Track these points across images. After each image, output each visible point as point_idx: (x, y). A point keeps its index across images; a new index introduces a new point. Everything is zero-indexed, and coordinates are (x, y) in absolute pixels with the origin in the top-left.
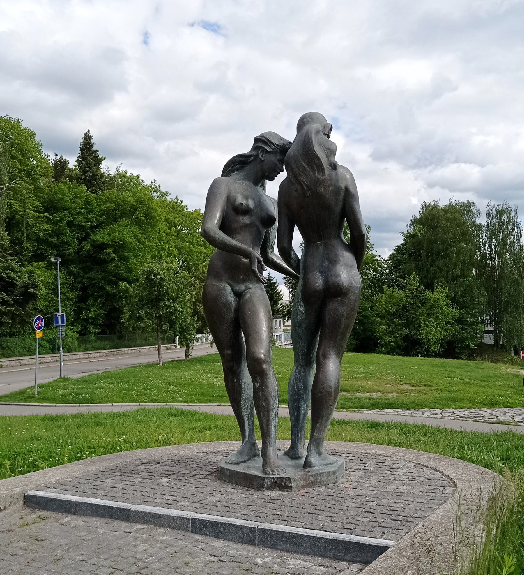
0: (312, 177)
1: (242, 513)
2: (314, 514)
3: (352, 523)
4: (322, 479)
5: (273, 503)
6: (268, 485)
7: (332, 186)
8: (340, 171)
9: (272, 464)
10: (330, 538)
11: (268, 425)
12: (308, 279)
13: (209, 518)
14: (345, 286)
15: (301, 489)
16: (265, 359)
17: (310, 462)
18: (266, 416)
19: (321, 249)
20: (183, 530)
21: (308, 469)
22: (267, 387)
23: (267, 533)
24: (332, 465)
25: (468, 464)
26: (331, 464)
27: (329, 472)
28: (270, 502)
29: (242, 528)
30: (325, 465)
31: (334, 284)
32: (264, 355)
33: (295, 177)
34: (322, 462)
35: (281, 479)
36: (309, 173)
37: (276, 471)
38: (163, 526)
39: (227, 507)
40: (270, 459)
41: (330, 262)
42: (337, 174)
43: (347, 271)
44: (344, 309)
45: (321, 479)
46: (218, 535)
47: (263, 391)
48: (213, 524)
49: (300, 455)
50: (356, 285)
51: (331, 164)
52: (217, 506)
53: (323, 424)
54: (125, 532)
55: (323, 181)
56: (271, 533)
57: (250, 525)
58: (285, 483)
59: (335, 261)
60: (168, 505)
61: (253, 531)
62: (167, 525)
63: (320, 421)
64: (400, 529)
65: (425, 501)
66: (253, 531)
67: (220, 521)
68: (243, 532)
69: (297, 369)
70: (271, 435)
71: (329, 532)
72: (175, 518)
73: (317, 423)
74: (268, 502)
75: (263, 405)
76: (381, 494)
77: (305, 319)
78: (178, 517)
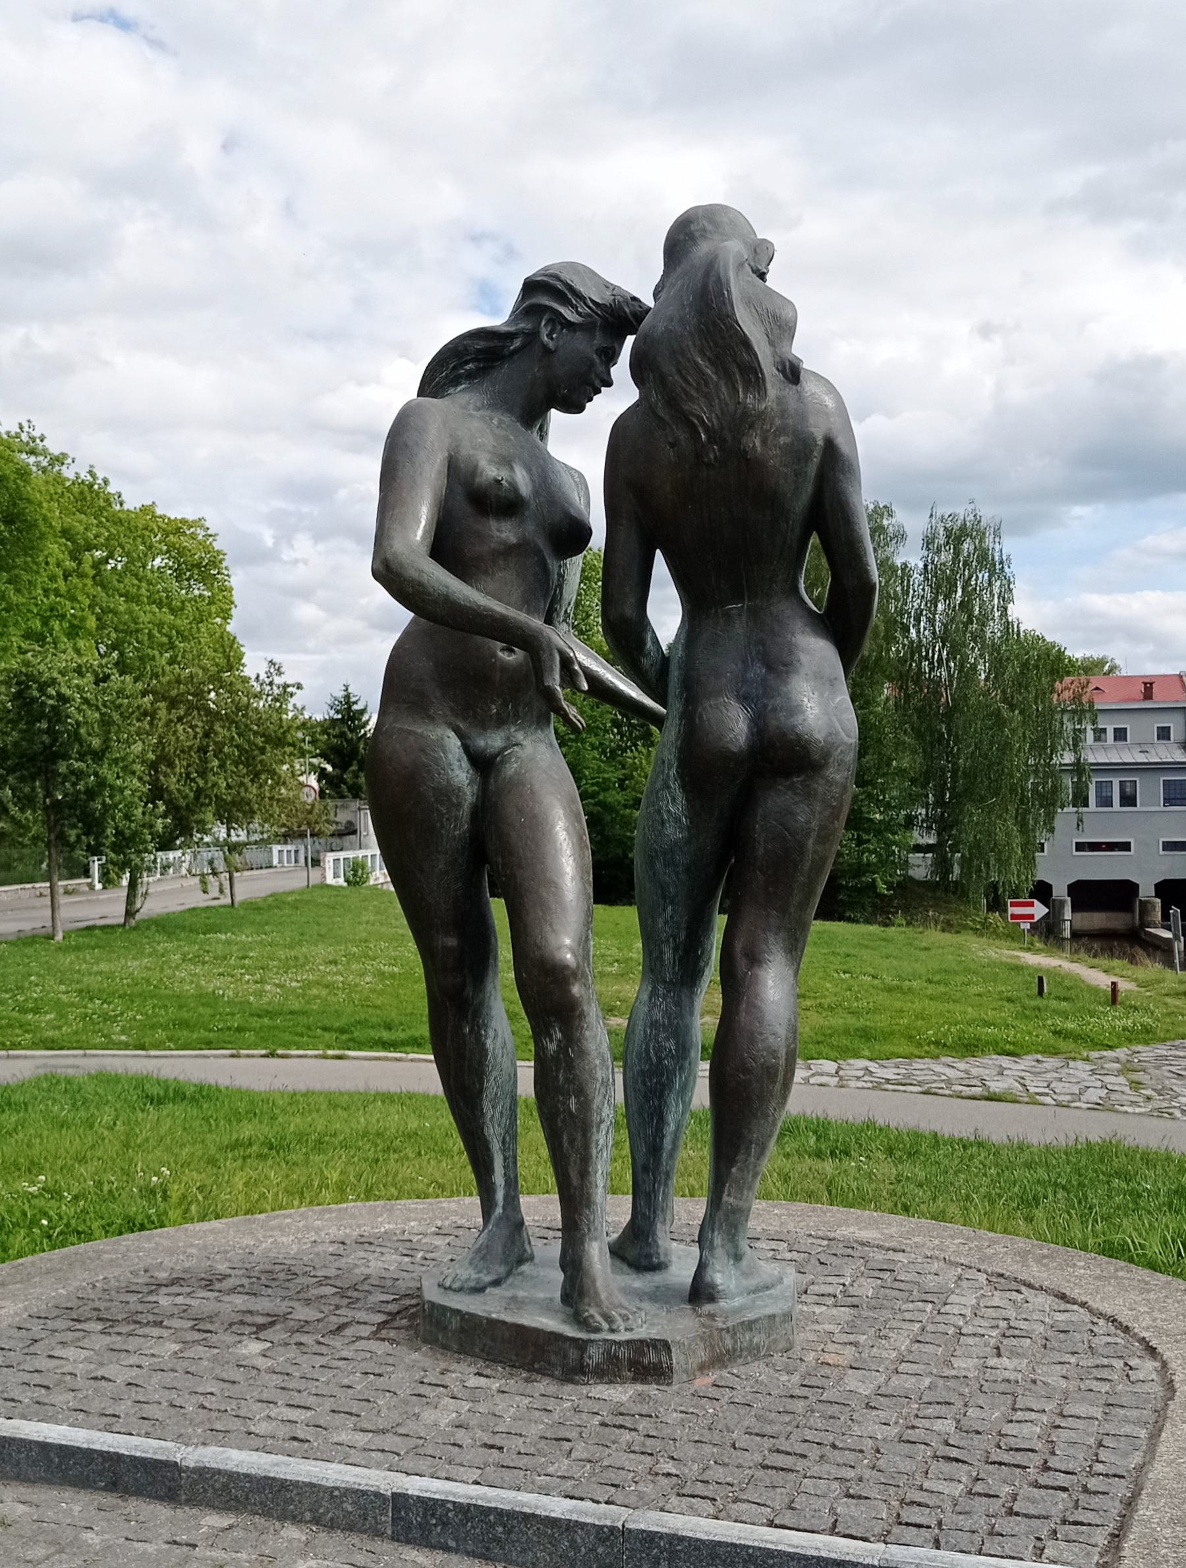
0: (727, 405)
1: (551, 1470)
2: (782, 1469)
3: (919, 1504)
4: (755, 1340)
5: (631, 1430)
6: (597, 1364)
7: (787, 434)
8: (809, 387)
9: (603, 1297)
10: (876, 1563)
11: (584, 1174)
12: (701, 717)
13: (454, 1495)
14: (817, 741)
15: (698, 1373)
16: (578, 967)
17: (713, 1286)
18: (579, 1143)
19: (740, 628)
20: (365, 1532)
21: (708, 1308)
22: (582, 1053)
23: (658, 1547)
24: (772, 1291)
25: (1145, 1273)
26: (768, 1288)
27: (774, 1316)
28: (621, 1427)
29: (569, 1527)
30: (754, 1292)
31: (784, 734)
32: (574, 954)
33: (672, 402)
34: (745, 1283)
35: (640, 1346)
36: (717, 386)
37: (619, 1321)
38: (296, 1519)
39: (492, 1447)
40: (594, 1282)
41: (770, 668)
42: (800, 398)
43: (821, 695)
44: (813, 813)
45: (751, 1340)
46: (488, 1549)
47: (570, 1066)
48: (468, 1512)
49: (662, 1258)
50: (846, 739)
51: (784, 367)
52: (460, 1446)
53: (751, 1167)
54: (175, 1543)
55: (761, 415)
56: (671, 1544)
57: (599, 1519)
58: (651, 1357)
59: (785, 665)
60: (298, 1444)
61: (608, 1539)
62: (308, 1516)
63: (740, 1157)
64: (1082, 1524)
65: (1098, 1412)
66: (608, 1539)
67: (493, 1505)
68: (573, 1542)
69: (653, 994)
70: (595, 1203)
71: (865, 1540)
72: (336, 1493)
73: (731, 1162)
74: (614, 1426)
75: (570, 1112)
76: (949, 1389)
77: (688, 841)
78: (347, 1490)
